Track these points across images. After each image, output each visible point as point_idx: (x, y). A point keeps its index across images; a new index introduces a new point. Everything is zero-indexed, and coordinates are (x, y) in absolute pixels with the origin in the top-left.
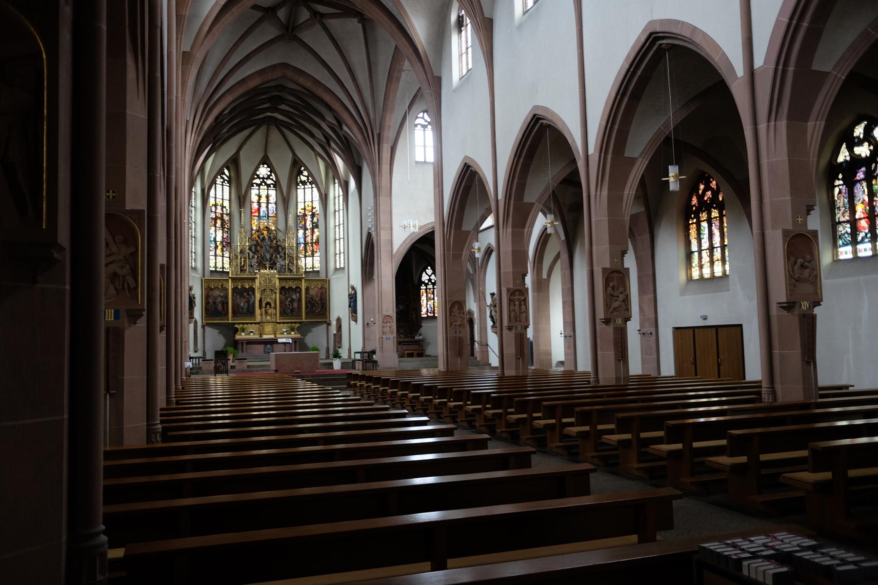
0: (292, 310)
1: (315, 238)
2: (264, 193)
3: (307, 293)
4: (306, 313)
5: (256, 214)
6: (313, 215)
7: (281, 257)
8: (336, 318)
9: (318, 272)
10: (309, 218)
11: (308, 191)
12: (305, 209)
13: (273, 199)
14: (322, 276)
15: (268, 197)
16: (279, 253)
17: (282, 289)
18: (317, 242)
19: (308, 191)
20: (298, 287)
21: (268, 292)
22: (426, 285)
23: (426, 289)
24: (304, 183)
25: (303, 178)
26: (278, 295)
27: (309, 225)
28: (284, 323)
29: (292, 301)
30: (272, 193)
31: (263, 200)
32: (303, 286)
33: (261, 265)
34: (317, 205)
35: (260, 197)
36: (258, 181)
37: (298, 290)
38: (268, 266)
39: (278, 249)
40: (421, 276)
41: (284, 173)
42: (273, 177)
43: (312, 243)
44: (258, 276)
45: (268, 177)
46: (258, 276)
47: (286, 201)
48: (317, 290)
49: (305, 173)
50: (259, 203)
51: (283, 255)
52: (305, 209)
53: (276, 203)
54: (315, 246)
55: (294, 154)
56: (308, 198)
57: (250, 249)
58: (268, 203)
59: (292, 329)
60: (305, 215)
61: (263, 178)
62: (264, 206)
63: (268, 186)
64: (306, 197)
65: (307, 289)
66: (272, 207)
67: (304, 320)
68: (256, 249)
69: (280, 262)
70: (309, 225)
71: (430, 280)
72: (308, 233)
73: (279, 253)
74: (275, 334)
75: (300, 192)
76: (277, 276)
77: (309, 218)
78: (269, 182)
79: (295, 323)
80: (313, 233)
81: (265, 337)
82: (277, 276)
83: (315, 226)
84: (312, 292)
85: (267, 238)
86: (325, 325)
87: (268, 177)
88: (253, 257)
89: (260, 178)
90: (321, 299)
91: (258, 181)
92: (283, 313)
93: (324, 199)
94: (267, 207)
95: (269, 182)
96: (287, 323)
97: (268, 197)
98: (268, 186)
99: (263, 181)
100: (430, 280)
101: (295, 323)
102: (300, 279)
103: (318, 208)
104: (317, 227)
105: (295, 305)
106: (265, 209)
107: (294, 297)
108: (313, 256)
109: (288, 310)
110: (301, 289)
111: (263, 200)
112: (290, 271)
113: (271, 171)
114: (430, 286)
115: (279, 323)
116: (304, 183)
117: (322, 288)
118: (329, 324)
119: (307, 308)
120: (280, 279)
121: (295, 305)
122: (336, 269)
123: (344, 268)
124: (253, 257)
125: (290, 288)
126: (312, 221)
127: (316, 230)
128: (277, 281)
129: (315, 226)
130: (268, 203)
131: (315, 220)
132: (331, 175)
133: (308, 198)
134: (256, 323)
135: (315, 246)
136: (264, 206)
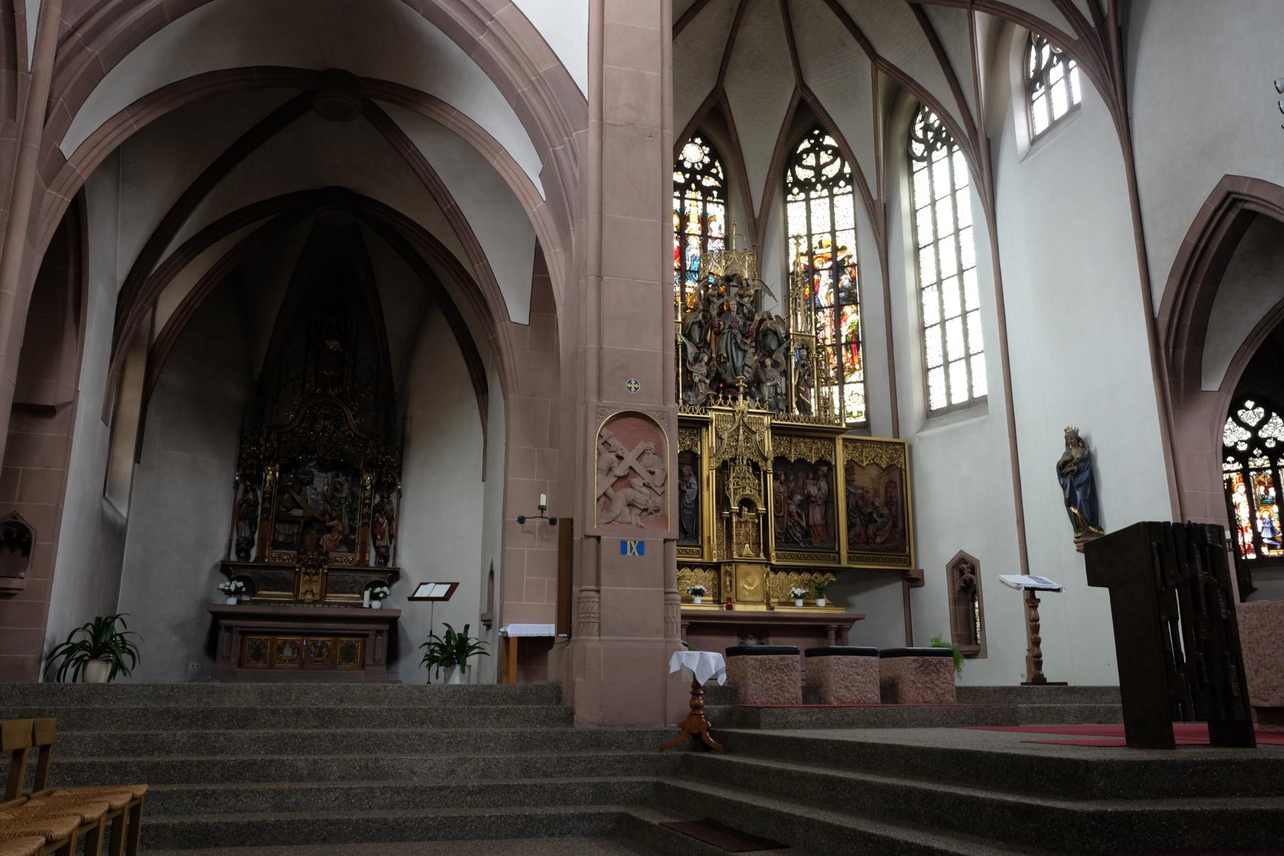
0: (808, 532)
1: (845, 330)
2: (694, 210)
3: (849, 482)
4: (850, 544)
5: (676, 264)
6: (838, 270)
7: (776, 364)
8: (949, 555)
9: (865, 427)
10: (825, 279)
11: (820, 207)
12: (810, 254)
13: (717, 228)
14: (883, 433)
15: (704, 220)
16: (770, 353)
17: (780, 461)
18: (855, 343)
19: (820, 207)
20: (822, 462)
21: (743, 468)
22: (1242, 457)
23: (1245, 473)
24: (806, 186)
25: (802, 174)
26: (770, 478)
27: (825, 295)
28: (787, 570)
29: (808, 501)
30: (716, 211)
31: (694, 227)
32: (841, 458)
33: (723, 387)
34: (847, 240)
35: (684, 219)
36: (679, 178)
37: (824, 468)
38: (742, 385)
39: (766, 338)
40: (1221, 432)
41: (758, 146)
42: (718, 168)
43: (837, 347)
44: (712, 415)
45: (706, 171)
46: (712, 415)
47: (758, 227)
48: (874, 472)
49: (810, 160)
50: (682, 235)
51: (779, 356)
52: (810, 254)
53: (727, 240)
54: (846, 355)
55: (802, 85)
56: (821, 223)
57: (688, 335)
58: (705, 237)
59: (820, 592)
60: (811, 270)
61: (693, 171)
62: (694, 242)
63: (706, 192)
64: (820, 220)
65: (849, 468)
66: (715, 246)
67: (844, 563)
68: (703, 339)
69: (773, 382)
70: (825, 295)
71: (1256, 442)
72: (825, 318)
73: (770, 353)
74: (768, 604)
75: (795, 211)
76: (767, 420)
77: (825, 279)
78: (708, 182)
79: (822, 571)
80: (838, 318)
81: (739, 608)
82: (767, 420)
83: (845, 298)
84: (865, 479)
85: (734, 308)
86: (898, 587)
87: (706, 171)
88: (697, 359)
89: (684, 171)
90: (889, 502)
91: (679, 178)
92: (785, 540)
93: (879, 216)
94: (703, 246)
95: (708, 182)
96: (799, 570)
97: (704, 220)
98: (706, 192)
99: (692, 179)
100: (1256, 442)
101: (822, 571)
102: (826, 433)
103: (851, 250)
104: (851, 299)
105: (816, 515)
106: (697, 253)
107: (813, 490)
108: (842, 382)
109: (799, 536)
110: (831, 468)
111: (694, 227)
112: (804, 407)
113: (714, 155)
114: (1263, 462)
115: (775, 569)
116: (806, 186)
117: (890, 467)
118: (913, 580)
119: (850, 526)
120: (776, 430)
121: (816, 515)
122: (930, 414)
123: (975, 404)
124: (697, 359)
125: (801, 461)
126: (835, 285)
127: (848, 310)
128: (767, 436)
129: (845, 298)
130: (705, 237)
131: (845, 281)
132: (899, 151)
133: (821, 223)
134: (704, 567)
135: (846, 355)
136: (694, 242)
